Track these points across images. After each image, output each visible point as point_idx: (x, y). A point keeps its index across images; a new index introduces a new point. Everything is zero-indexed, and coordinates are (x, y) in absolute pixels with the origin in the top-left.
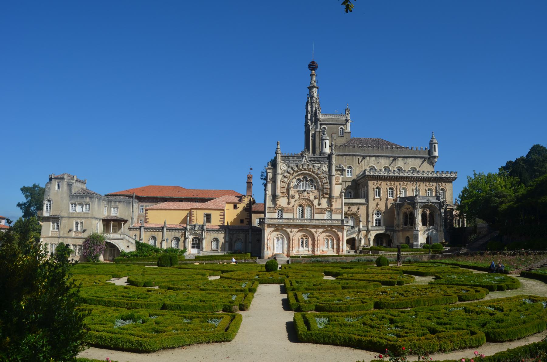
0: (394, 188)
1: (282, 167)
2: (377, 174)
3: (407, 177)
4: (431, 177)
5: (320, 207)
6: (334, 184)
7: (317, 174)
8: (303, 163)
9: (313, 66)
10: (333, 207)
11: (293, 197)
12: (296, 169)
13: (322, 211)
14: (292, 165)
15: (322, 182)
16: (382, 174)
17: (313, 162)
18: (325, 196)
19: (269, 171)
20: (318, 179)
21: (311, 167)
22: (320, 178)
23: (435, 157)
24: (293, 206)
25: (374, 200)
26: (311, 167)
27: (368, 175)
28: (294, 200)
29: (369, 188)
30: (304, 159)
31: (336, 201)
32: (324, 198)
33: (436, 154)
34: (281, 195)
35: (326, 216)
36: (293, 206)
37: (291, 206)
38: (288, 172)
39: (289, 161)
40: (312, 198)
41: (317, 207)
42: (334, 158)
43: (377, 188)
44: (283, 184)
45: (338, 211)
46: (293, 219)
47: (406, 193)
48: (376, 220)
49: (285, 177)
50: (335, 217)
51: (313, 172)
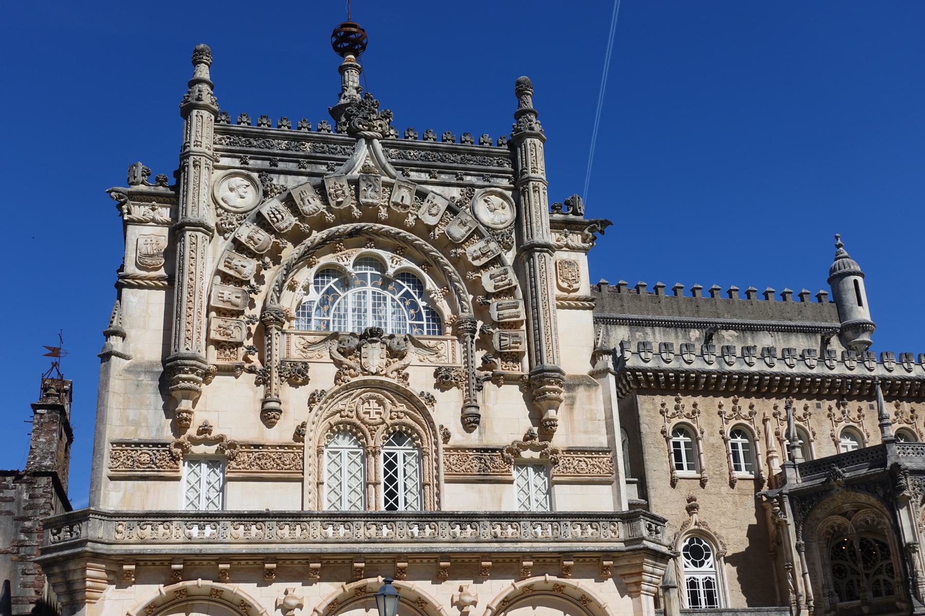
0: (756, 424)
1: (222, 192)
2: (673, 365)
3: (804, 377)
4: (904, 380)
5: (473, 439)
6: (553, 302)
7: (448, 244)
8: (356, 174)
9: (348, 41)
10: (559, 441)
11: (297, 375)
12: (312, 204)
13: (490, 464)
14: (290, 182)
15: (475, 286)
16: (698, 365)
17: (414, 176)
18: (501, 366)
19: (139, 211)
20: (451, 268)
21: (405, 195)
22: (458, 261)
23: (860, 327)
24: (299, 435)
25: (673, 484)
26: (405, 195)
27: (633, 370)
28: (304, 392)
29: (644, 428)
30: (362, 156)
31: (571, 405)
32: (498, 379)
33: (863, 314)
34: (213, 358)
35: (520, 492)
36: (299, 435)
37: (282, 433)
38: (261, 221)
39: (272, 158)
40: (420, 380)
41: (459, 437)
42: (535, 155)
43: (679, 430)
44: (230, 292)
45: (584, 465)
46: (296, 517)
47: (806, 448)
48: (693, 584)
49: (239, 247)
50: (570, 499)
51: (425, 230)
